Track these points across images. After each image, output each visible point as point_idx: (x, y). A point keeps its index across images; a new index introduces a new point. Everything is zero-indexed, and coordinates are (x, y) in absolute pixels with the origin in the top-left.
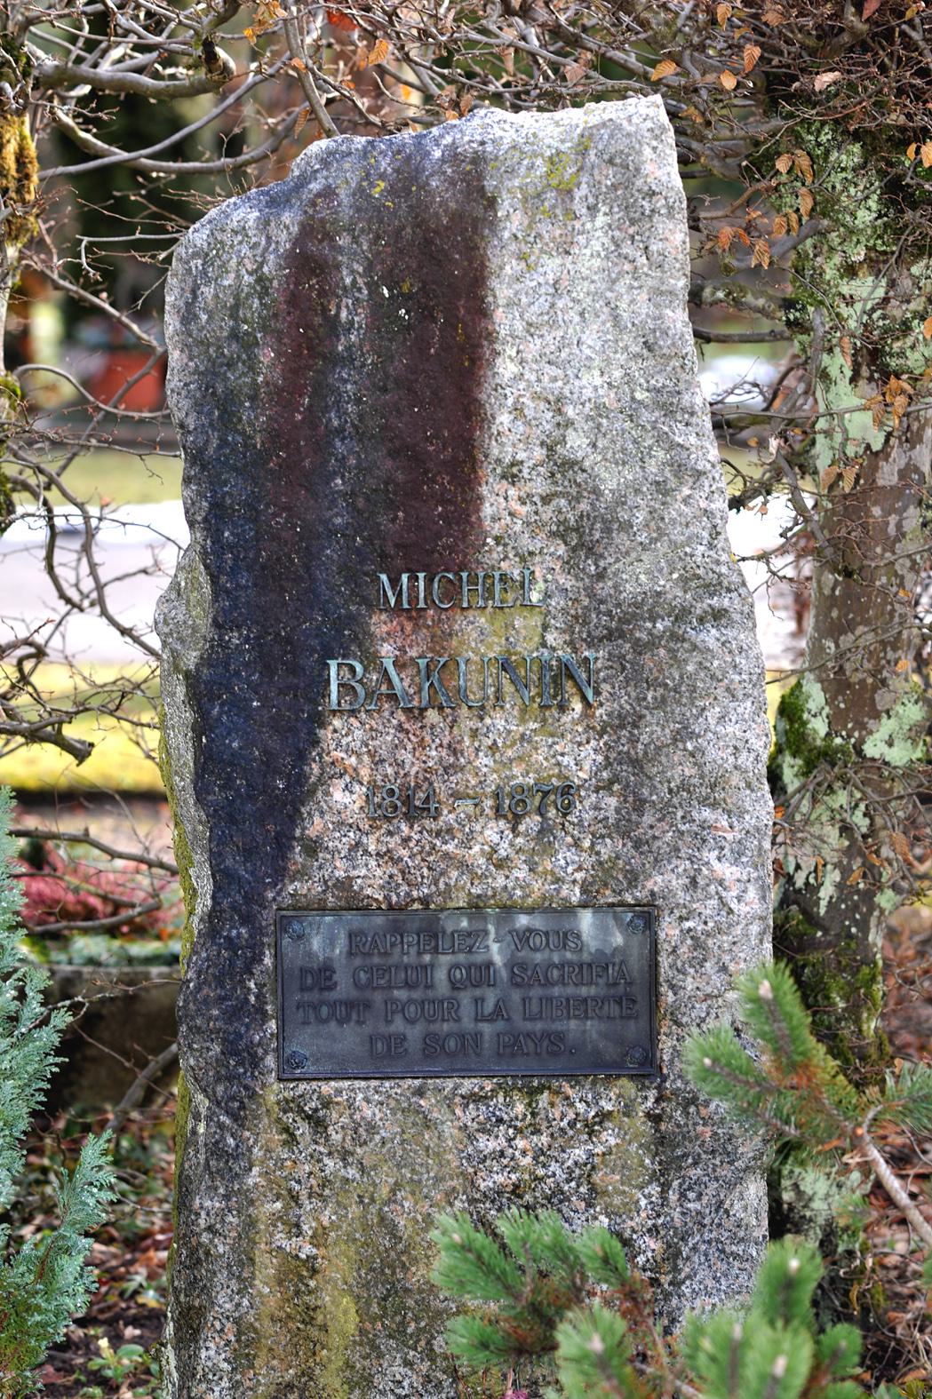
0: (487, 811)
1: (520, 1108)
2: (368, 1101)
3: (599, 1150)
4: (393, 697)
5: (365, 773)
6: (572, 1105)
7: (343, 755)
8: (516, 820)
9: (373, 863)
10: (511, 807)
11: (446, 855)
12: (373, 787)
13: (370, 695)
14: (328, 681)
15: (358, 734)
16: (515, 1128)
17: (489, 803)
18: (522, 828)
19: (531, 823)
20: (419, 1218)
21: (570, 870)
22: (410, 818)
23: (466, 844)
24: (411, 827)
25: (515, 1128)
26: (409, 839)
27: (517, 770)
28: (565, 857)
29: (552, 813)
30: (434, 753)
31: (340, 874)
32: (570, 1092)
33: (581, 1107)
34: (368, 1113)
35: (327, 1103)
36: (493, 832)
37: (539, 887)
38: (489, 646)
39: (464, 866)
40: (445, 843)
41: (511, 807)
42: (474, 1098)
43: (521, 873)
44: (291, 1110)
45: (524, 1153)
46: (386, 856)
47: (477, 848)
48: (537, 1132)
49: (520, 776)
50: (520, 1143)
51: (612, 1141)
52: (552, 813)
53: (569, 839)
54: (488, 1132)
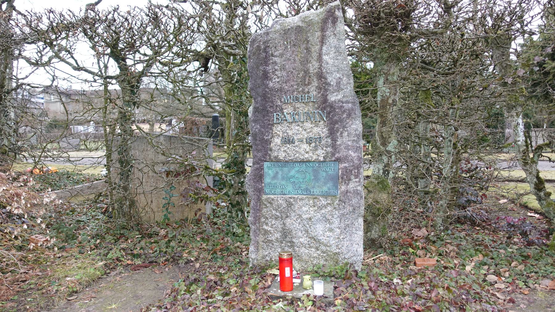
1: (311, 202)
3: (327, 211)
4: (286, 120)
5: (281, 135)
8: (310, 144)
10: (309, 141)
11: (296, 151)
13: (282, 120)
17: (305, 140)
19: (313, 145)
27: (311, 134)
29: (317, 143)
31: (276, 155)
33: (323, 202)
34: (280, 201)
35: (273, 200)
36: (305, 146)
37: (315, 157)
39: (300, 153)
42: (302, 199)
43: (311, 154)
46: (285, 151)
48: (314, 206)
49: (311, 135)
50: (311, 209)
52: (317, 143)
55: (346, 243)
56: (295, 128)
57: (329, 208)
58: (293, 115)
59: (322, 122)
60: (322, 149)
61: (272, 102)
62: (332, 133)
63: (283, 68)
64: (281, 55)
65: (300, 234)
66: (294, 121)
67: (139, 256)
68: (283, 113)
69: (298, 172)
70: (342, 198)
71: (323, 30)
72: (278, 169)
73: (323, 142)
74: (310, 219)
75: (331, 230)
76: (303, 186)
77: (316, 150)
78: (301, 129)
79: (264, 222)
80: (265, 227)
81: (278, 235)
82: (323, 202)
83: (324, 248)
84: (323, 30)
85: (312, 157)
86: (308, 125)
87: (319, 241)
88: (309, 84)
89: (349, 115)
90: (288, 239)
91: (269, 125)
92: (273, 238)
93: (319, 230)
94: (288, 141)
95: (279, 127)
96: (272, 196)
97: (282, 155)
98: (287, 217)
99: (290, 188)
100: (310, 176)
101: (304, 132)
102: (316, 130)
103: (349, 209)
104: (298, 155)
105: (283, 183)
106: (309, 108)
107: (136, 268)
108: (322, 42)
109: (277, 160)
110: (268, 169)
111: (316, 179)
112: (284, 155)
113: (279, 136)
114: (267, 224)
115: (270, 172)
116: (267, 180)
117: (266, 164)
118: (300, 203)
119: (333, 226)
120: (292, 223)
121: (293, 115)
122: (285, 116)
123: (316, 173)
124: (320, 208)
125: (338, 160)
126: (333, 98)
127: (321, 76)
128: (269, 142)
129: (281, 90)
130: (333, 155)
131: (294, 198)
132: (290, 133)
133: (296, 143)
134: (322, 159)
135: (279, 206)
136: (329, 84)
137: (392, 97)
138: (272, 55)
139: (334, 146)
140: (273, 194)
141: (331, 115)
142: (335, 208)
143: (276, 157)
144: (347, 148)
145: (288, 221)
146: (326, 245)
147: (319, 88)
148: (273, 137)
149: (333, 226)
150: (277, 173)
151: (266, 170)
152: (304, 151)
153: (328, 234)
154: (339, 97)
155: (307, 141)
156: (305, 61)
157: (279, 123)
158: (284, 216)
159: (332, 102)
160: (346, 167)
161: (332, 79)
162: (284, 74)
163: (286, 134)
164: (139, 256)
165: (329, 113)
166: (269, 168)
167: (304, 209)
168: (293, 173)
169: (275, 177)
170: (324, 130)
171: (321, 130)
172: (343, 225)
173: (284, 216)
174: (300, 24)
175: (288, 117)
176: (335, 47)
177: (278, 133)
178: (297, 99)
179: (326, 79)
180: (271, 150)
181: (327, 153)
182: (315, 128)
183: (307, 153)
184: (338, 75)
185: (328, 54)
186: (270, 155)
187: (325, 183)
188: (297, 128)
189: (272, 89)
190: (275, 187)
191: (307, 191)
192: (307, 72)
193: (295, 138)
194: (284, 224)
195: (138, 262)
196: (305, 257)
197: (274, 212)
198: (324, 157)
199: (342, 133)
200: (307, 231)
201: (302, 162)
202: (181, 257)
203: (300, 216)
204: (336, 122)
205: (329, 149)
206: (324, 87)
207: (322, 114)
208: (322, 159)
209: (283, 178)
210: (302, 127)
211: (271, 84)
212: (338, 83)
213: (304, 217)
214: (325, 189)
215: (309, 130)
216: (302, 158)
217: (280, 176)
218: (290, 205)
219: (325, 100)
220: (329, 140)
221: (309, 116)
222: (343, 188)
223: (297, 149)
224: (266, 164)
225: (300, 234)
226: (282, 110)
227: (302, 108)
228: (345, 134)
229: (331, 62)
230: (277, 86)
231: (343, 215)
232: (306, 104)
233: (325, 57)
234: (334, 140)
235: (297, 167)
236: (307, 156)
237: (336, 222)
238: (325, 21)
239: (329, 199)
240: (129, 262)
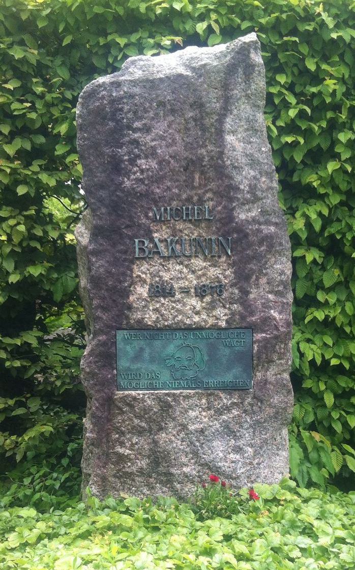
0: (192, 294)
1: (204, 401)
2: (149, 398)
3: (231, 416)
4: (158, 253)
5: (148, 280)
6: (222, 400)
7: (140, 274)
9: (151, 313)
10: (201, 292)
11: (178, 310)
12: (151, 285)
13: (150, 253)
14: (135, 248)
15: (146, 266)
16: (202, 408)
17: (193, 290)
18: (204, 300)
19: (208, 299)
20: (167, 440)
21: (222, 315)
22: (165, 297)
23: (184, 305)
24: (165, 300)
25: (202, 408)
26: (164, 304)
27: (203, 279)
28: (220, 312)
30: (173, 273)
32: (222, 395)
33: (225, 401)
34: (149, 402)
35: (135, 399)
36: (194, 302)
37: (211, 321)
38: (193, 234)
40: (177, 305)
42: (187, 397)
44: (122, 401)
45: (205, 417)
46: (156, 310)
47: (188, 307)
50: (204, 414)
51: (236, 413)
53: (221, 305)
54: (192, 410)
56: (175, 268)
57: (235, 412)
58: (171, 243)
59: (223, 259)
60: (224, 307)
61: (131, 218)
62: (243, 278)
65: (184, 460)
66: (174, 256)
68: (152, 240)
69: (180, 348)
70: (259, 393)
72: (142, 343)
73: (225, 295)
74: (202, 431)
75: (238, 450)
76: (190, 374)
77: (214, 308)
78: (185, 270)
79: (117, 440)
80: (121, 450)
81: (143, 463)
82: (226, 400)
85: (205, 321)
86: (198, 263)
90: (161, 469)
91: (125, 260)
92: (134, 469)
94: (161, 291)
95: (145, 267)
96: (133, 393)
97: (150, 318)
98: (161, 429)
101: (190, 276)
102: (213, 272)
104: (180, 317)
105: (154, 367)
109: (141, 327)
112: (154, 317)
113: (145, 281)
114: (122, 444)
115: (128, 348)
117: (120, 335)
118: (185, 404)
119: (241, 443)
120: (170, 439)
121: (171, 243)
122: (156, 246)
123: (212, 350)
124: (219, 412)
128: (126, 293)
131: (174, 395)
132: (166, 276)
133: (178, 296)
134: (223, 324)
135: (146, 410)
136: (237, 189)
138: (129, 127)
140: (135, 389)
141: (236, 244)
142: (245, 411)
143: (140, 321)
146: (230, 477)
148: (133, 283)
149: (241, 443)
150: (142, 350)
151: (120, 345)
152: (192, 310)
153: (232, 456)
155: (196, 292)
157: (144, 259)
158: (155, 428)
159: (242, 221)
160: (265, 339)
162: (154, 164)
163: (157, 279)
166: (126, 341)
167: (192, 414)
168: (171, 349)
169: (138, 357)
170: (228, 273)
172: (258, 441)
173: (155, 428)
174: (182, 70)
175: (162, 247)
177: (144, 276)
178: (178, 213)
179: (231, 178)
180: (130, 307)
181: (233, 314)
182: (212, 269)
183: (198, 313)
184: (252, 173)
185: (234, 132)
186: (127, 318)
187: (228, 369)
188: (178, 267)
189: (131, 193)
190: (137, 375)
191: (196, 383)
193: (176, 286)
194: (155, 442)
197: (136, 421)
198: (227, 322)
199: (257, 279)
200: (195, 454)
201: (189, 329)
203: (184, 427)
204: (250, 259)
206: (227, 193)
207: (225, 245)
208: (223, 324)
209: (152, 360)
210: (187, 266)
211: (127, 183)
212: (253, 189)
213: (192, 428)
214: (229, 378)
215: (200, 273)
216: (188, 322)
217: (146, 355)
218: (166, 407)
219: (230, 218)
220: (237, 291)
221: (200, 247)
223: (179, 306)
225: (184, 460)
226: (149, 234)
227: (189, 232)
229: (239, 146)
230: (142, 188)
231: (258, 422)
232: (197, 223)
233: (229, 138)
236: (196, 319)
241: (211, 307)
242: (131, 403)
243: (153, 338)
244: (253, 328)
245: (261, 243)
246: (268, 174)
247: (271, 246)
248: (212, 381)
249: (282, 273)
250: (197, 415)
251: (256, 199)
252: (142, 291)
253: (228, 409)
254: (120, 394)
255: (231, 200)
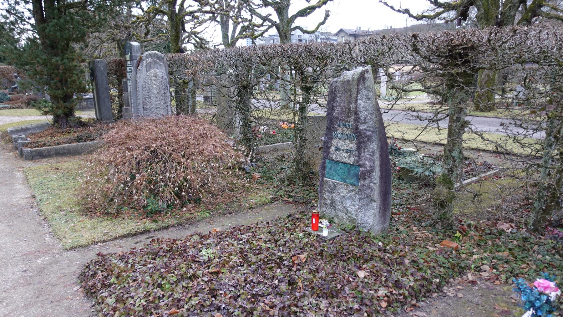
10: (347, 151)
19: (349, 154)
28: (352, 159)
37: (349, 161)
41: (347, 151)
42: (340, 184)
55: (361, 215)
57: (354, 193)
62: (359, 149)
63: (340, 106)
64: (340, 97)
65: (339, 204)
67: (291, 197)
69: (341, 168)
70: (360, 188)
71: (358, 85)
74: (344, 196)
75: (354, 205)
77: (350, 157)
80: (324, 196)
81: (329, 202)
82: (351, 188)
83: (349, 214)
84: (358, 85)
86: (347, 142)
87: (347, 210)
88: (350, 117)
89: (369, 139)
93: (348, 203)
94: (337, 149)
99: (337, 177)
100: (346, 172)
102: (351, 145)
103: (364, 195)
106: (347, 132)
107: (287, 203)
108: (358, 93)
109: (332, 160)
110: (328, 164)
111: (349, 174)
116: (327, 170)
118: (340, 186)
123: (349, 170)
124: (350, 191)
125: (360, 166)
126: (362, 127)
127: (356, 113)
128: (329, 148)
129: (338, 118)
130: (358, 162)
132: (339, 145)
134: (352, 163)
136: (359, 118)
137: (456, 115)
139: (359, 156)
143: (332, 158)
144: (366, 159)
145: (334, 195)
147: (355, 120)
151: (327, 164)
152: (344, 157)
153: (352, 207)
154: (365, 127)
156: (350, 103)
161: (362, 116)
164: (291, 197)
165: (358, 136)
167: (342, 190)
168: (339, 168)
169: (330, 169)
171: (353, 146)
172: (360, 204)
176: (366, 95)
184: (366, 113)
185: (362, 99)
187: (353, 178)
191: (344, 180)
192: (349, 109)
195: (291, 200)
196: (340, 217)
199: (364, 149)
201: (342, 163)
202: (310, 202)
204: (361, 143)
205: (356, 158)
206: (357, 120)
208: (352, 163)
212: (365, 118)
213: (341, 194)
214: (352, 181)
219: (357, 128)
222: (362, 183)
224: (328, 161)
225: (339, 204)
228: (366, 150)
229: (363, 104)
230: (336, 116)
232: (348, 129)
233: (359, 101)
234: (360, 153)
235: (341, 166)
236: (345, 160)
237: (357, 201)
238: (359, 79)
239: (354, 187)
240: (286, 199)
241: (350, 156)
242: (327, 182)
243: (335, 163)
244: (360, 166)
245: (366, 137)
246: (371, 114)
247: (369, 139)
248: (348, 181)
249: (373, 148)
250: (343, 191)
251: (366, 123)
252: (333, 148)
253: (352, 191)
254: (325, 179)
255: (358, 122)
